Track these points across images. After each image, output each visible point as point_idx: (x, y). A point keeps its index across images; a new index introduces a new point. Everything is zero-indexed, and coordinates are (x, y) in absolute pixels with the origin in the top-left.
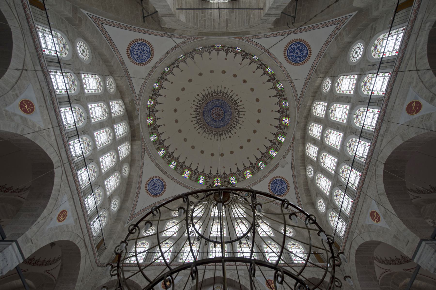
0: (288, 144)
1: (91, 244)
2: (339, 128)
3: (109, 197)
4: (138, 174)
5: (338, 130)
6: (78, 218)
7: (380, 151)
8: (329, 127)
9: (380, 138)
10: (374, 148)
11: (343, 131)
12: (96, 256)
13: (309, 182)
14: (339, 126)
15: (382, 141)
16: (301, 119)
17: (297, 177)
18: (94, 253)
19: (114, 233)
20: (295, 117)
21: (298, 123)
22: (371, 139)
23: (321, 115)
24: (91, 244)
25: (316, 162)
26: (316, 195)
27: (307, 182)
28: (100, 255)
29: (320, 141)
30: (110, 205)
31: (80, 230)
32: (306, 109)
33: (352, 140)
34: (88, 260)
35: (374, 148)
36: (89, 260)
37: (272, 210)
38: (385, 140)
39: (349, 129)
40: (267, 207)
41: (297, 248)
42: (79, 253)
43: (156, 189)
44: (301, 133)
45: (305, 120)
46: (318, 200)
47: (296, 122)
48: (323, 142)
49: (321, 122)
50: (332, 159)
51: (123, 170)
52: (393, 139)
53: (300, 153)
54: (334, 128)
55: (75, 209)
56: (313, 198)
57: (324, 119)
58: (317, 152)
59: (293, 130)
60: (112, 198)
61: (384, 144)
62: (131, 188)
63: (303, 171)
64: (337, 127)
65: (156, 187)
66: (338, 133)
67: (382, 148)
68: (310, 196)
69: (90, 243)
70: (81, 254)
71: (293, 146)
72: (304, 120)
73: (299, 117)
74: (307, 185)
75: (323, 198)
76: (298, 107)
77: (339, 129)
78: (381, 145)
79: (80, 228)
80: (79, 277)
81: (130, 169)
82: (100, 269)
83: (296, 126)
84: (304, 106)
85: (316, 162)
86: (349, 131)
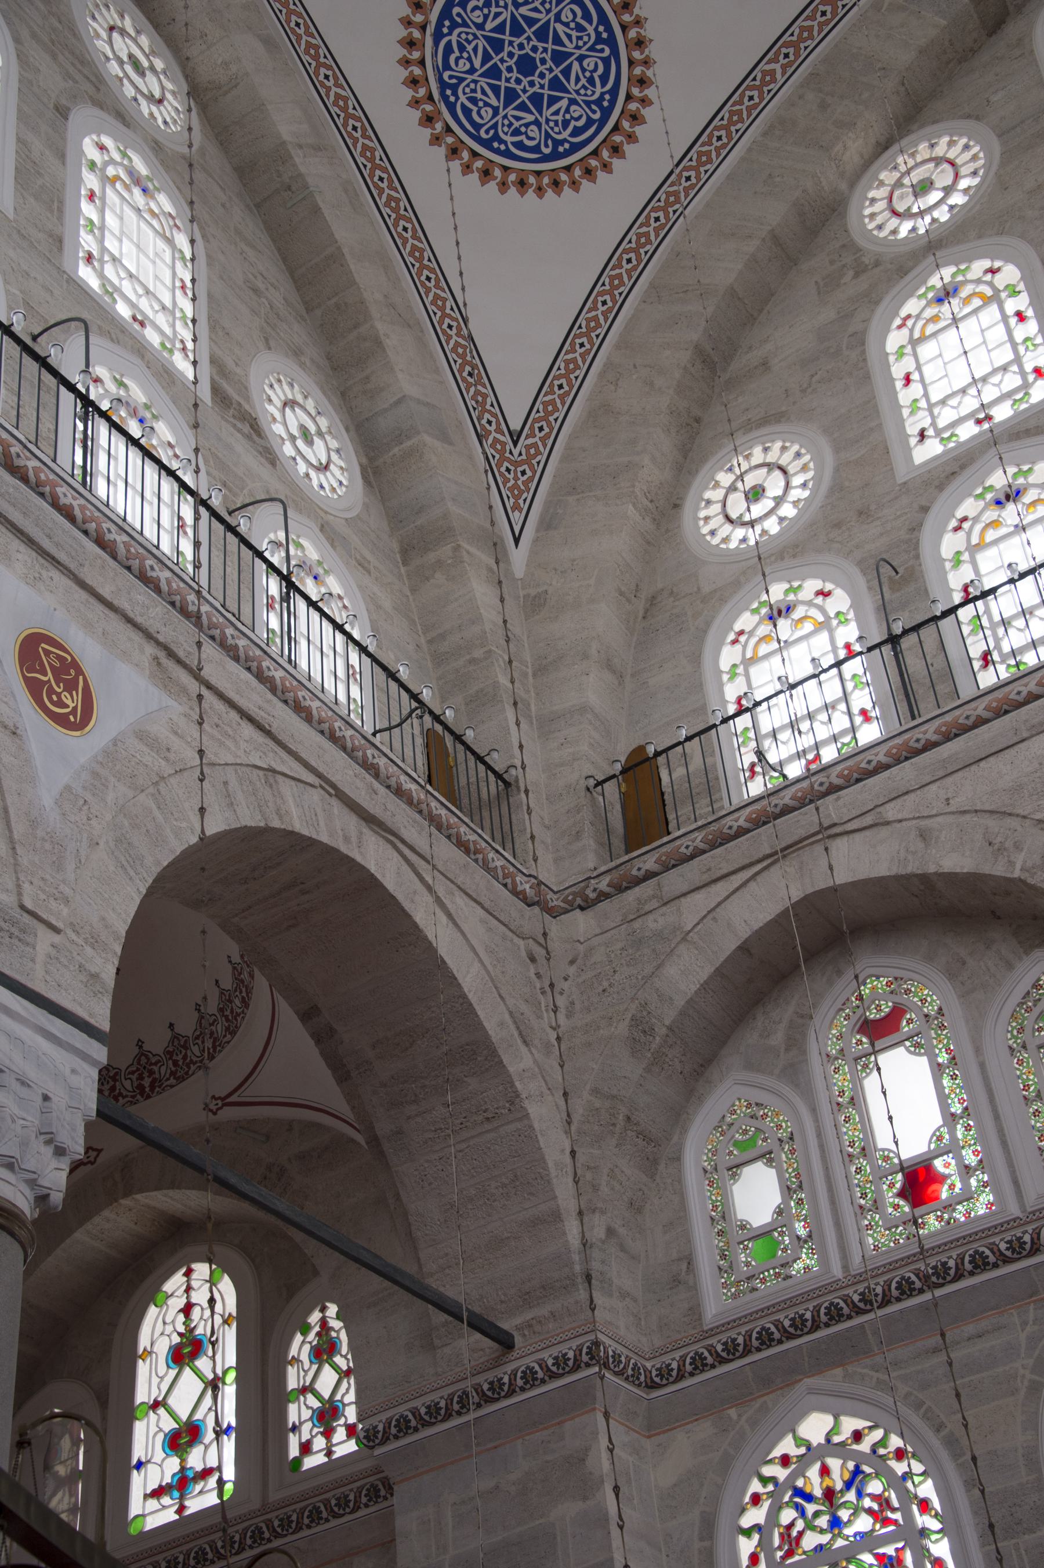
1: (399, 792)
3: (216, 390)
4: (269, 43)
6: (162, 655)
12: (492, 855)
18: (462, 845)
19: (478, 653)
24: (399, 792)
28: (506, 837)
30: (270, 456)
31: (247, 730)
34: (459, 903)
36: (460, 900)
42: (369, 884)
43: (540, 85)
51: (114, 68)
55: (84, 595)
60: (244, 390)
62: (316, 210)
65: (526, 65)
69: (382, 790)
70: (390, 883)
79: (234, 715)
80: (490, 1026)
81: (157, 26)
82: (582, 923)
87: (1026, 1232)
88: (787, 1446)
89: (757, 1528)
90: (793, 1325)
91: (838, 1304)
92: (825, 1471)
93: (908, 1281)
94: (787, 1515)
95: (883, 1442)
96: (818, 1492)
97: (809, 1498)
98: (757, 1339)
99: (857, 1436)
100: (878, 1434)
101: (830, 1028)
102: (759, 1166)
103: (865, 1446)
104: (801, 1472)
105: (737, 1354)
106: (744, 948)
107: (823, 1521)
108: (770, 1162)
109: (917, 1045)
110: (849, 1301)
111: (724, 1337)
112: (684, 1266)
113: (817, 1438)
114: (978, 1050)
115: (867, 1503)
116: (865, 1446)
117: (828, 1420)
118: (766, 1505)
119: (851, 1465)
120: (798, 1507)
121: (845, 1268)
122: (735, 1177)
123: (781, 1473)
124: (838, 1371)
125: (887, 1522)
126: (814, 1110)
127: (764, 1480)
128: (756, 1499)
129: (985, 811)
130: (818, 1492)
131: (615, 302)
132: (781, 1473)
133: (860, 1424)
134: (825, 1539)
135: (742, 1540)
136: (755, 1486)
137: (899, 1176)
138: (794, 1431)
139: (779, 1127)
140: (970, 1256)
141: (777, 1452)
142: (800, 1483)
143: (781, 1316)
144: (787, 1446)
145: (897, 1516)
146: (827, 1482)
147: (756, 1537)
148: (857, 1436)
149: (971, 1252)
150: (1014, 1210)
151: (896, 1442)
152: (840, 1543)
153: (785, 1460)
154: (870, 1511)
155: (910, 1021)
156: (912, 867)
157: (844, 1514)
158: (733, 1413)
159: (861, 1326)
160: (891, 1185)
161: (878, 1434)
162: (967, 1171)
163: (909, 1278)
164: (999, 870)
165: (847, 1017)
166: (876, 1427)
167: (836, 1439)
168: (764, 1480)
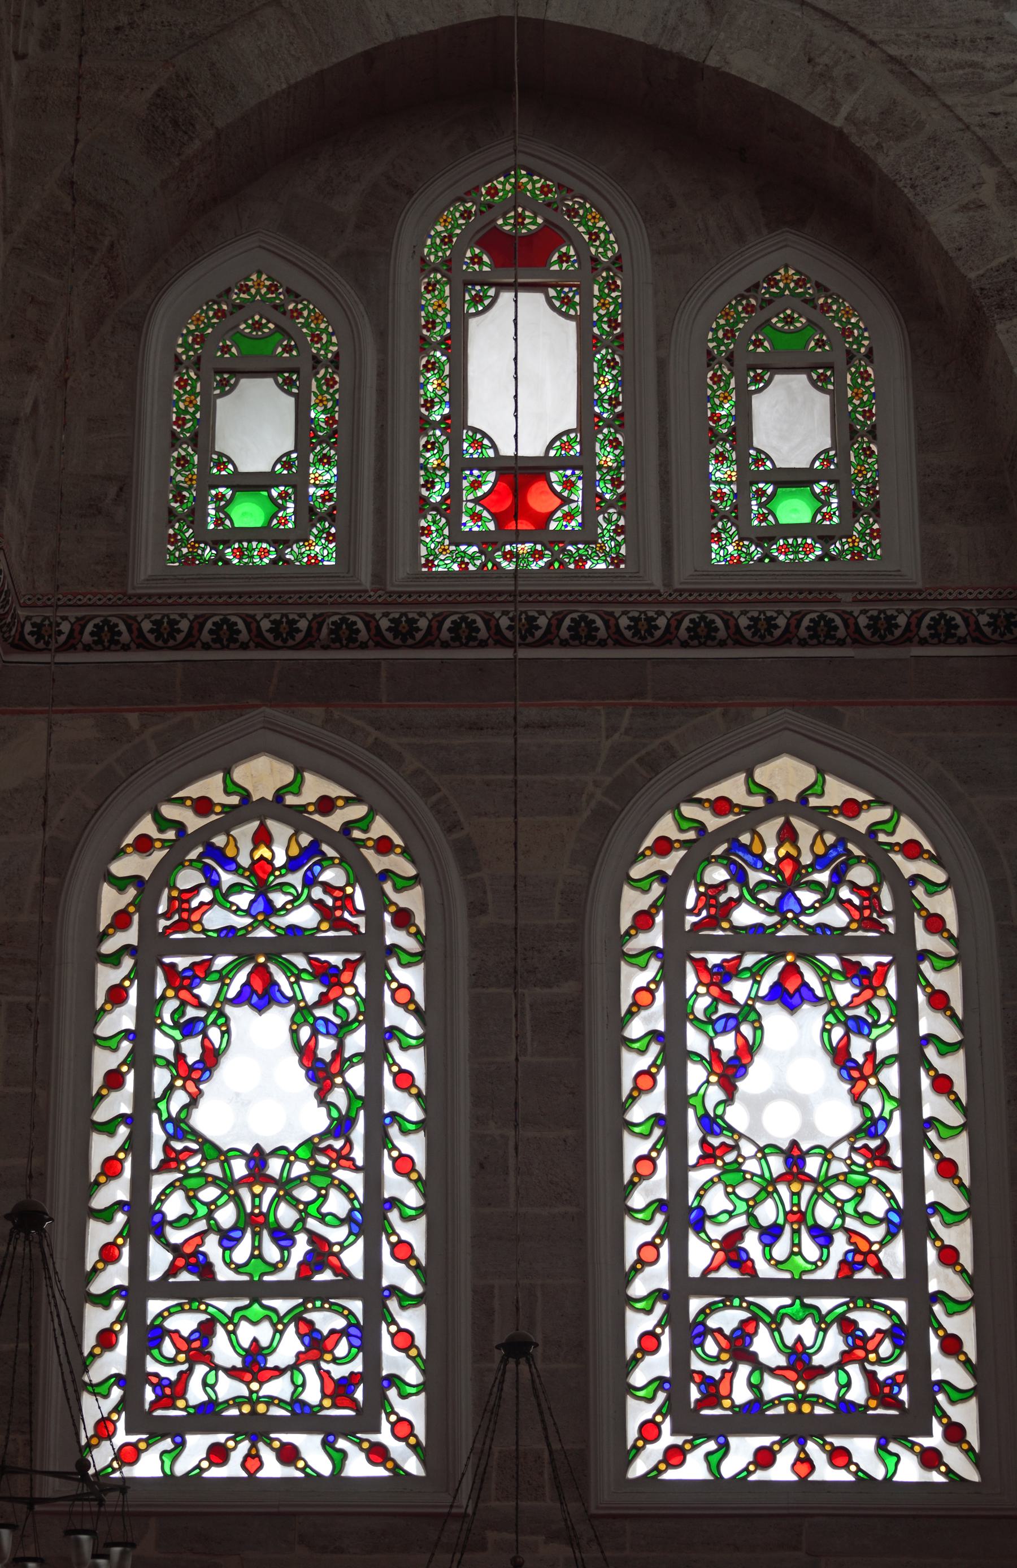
87: (663, 613)
88: (212, 787)
89: (137, 881)
90: (275, 629)
91: (355, 623)
92: (263, 837)
93: (472, 627)
94: (188, 878)
95: (364, 823)
96: (244, 861)
97: (228, 863)
98: (211, 631)
99: (326, 805)
100: (358, 811)
101: (436, 221)
102: (267, 385)
103: (334, 821)
104: (224, 827)
105: (171, 643)
106: (369, 57)
107: (243, 900)
108: (286, 386)
109: (567, 301)
110: (372, 625)
111: (157, 613)
112: (113, 490)
113: (263, 790)
114: (662, 339)
115: (317, 893)
116: (334, 821)
117: (286, 773)
118: (158, 855)
119: (305, 839)
120: (207, 871)
121: (379, 577)
122: (226, 388)
123: (193, 822)
124: (319, 712)
125: (339, 924)
126: (382, 335)
127: (162, 823)
128: (144, 844)
129: (815, 9)
130: (244, 861)
132: (193, 822)
133: (335, 791)
134: (241, 922)
135: (107, 891)
136: (146, 826)
137: (491, 476)
138: (228, 772)
139: (316, 338)
140: (573, 620)
141: (194, 791)
142: (219, 841)
143: (259, 613)
144: (212, 787)
145: (360, 921)
146: (264, 852)
147: (132, 892)
148: (326, 805)
149: (575, 615)
150: (655, 580)
151: (380, 828)
152: (263, 933)
153: (202, 806)
154: (318, 905)
155: (564, 258)
156: (681, 45)
157: (279, 899)
158: (133, 719)
159: (376, 663)
160: (476, 485)
161: (358, 811)
162: (593, 503)
163: (474, 621)
164: (815, 105)
165: (466, 214)
166: (358, 800)
167: (290, 800)
168: (162, 823)
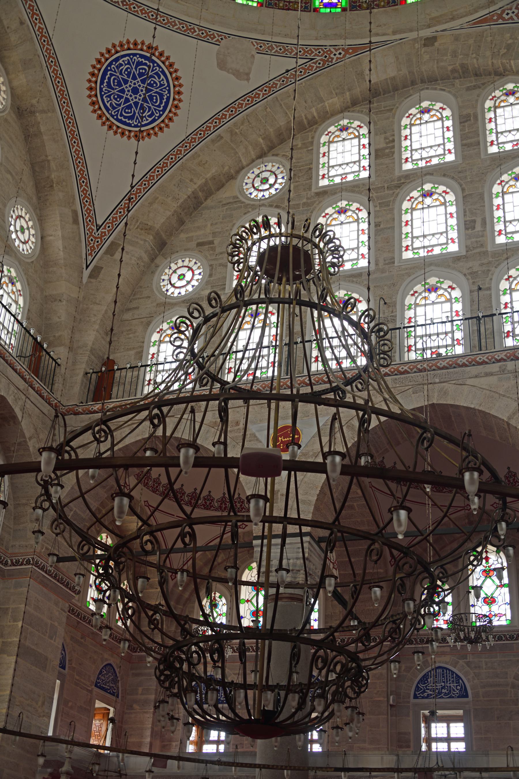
0: (326, 37)
2: (474, 228)
5: (467, 229)
7: (460, 382)
8: (463, 190)
9: (495, 367)
10: (464, 365)
11: (468, 249)
13: (225, 194)
14: (478, 227)
15: (487, 375)
16: (455, 54)
17: (213, 141)
20: (453, 19)
21: (430, 41)
22: (483, 348)
23: (493, 137)
25: (314, 190)
26: (199, 244)
27: (221, 186)
29: (397, 174)
32: (498, 62)
33: (453, 289)
35: (464, 365)
37: (43, 128)
38: (493, 380)
39: (482, 265)
40: (34, 101)
41: (13, 297)
44: (393, 78)
45: (454, 71)
46: (191, 257)
47: (427, 33)
48: (398, 186)
49: (468, 145)
50: (358, 248)
52: (504, 396)
53: (314, 110)
54: (465, 212)
56: (183, 236)
57: (482, 156)
58: (350, 178)
59: (394, 33)
61: (483, 382)
63: (253, 154)
64: (474, 221)
66: (454, 234)
67: (470, 382)
68: (182, 222)
71: (327, 63)
72: (450, 68)
73: (457, 38)
74: (209, 194)
75: (211, 275)
76: (500, 16)
77: (470, 231)
78: (476, 377)
83: (415, 40)
84: (509, 47)
85: (314, 190)
86: (475, 265)
131: (190, 147)
